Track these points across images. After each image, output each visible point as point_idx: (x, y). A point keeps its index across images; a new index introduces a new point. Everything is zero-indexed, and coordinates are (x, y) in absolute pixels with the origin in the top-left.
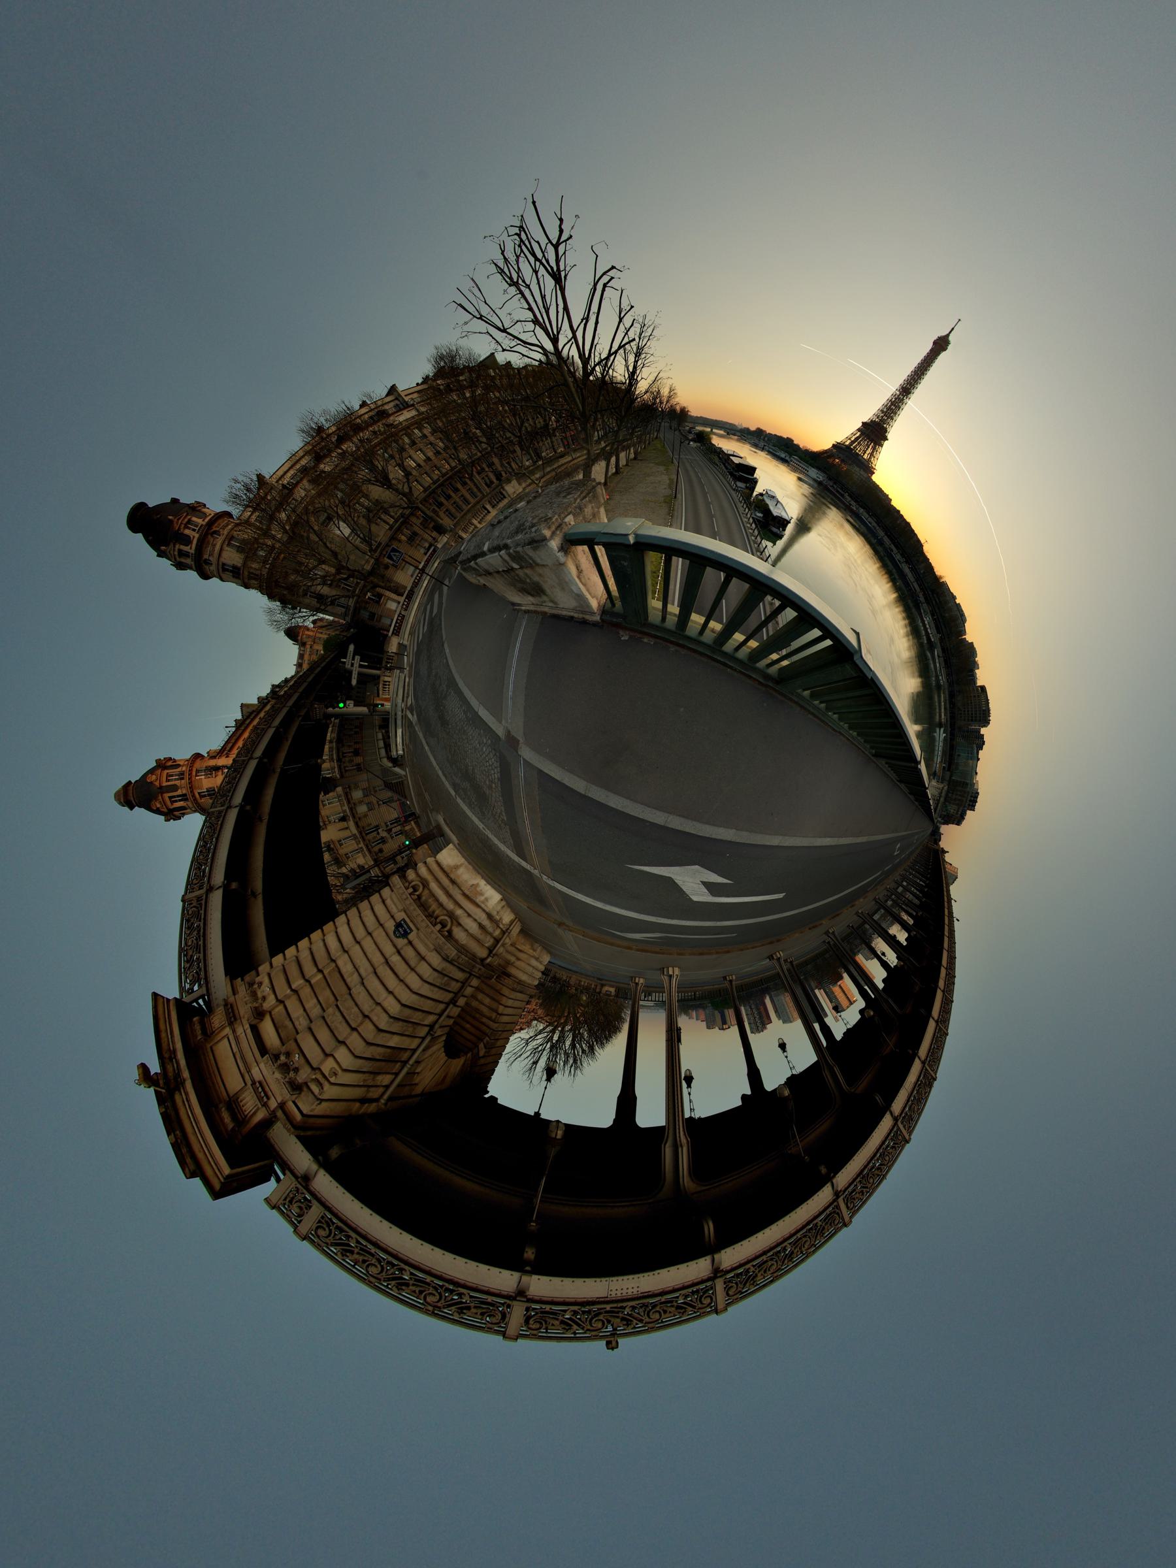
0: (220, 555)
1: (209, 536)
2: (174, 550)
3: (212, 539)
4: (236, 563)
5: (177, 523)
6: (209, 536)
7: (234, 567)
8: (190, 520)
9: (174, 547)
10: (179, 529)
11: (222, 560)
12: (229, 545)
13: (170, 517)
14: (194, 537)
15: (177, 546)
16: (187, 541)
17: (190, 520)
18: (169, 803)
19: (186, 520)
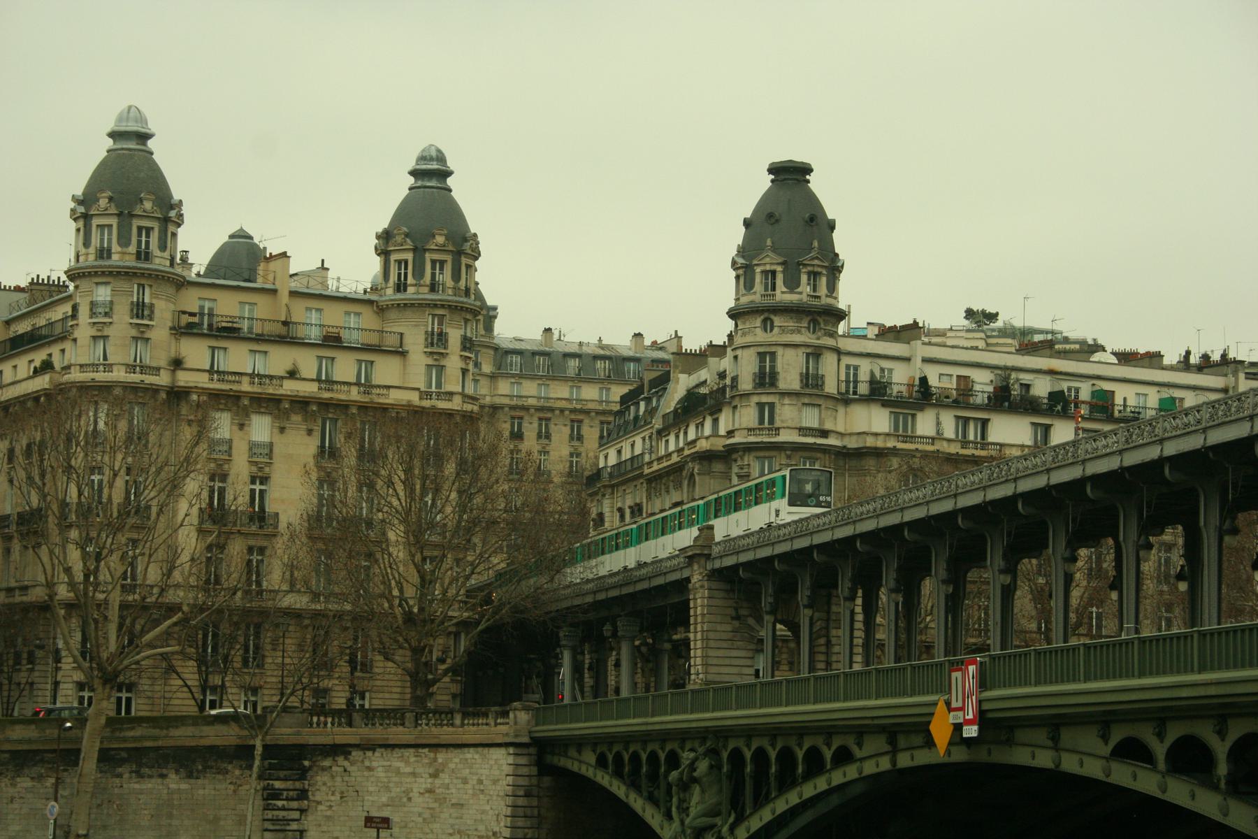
0: (786, 345)
1: (809, 318)
2: (771, 264)
3: (806, 325)
4: (781, 377)
5: (813, 259)
6: (809, 318)
7: (774, 376)
8: (820, 274)
9: (778, 264)
10: (805, 265)
11: (780, 351)
12: (808, 355)
13: (816, 244)
14: (801, 293)
15: (779, 268)
16: (792, 285)
17: (820, 274)
18: (436, 256)
19: (819, 270)
